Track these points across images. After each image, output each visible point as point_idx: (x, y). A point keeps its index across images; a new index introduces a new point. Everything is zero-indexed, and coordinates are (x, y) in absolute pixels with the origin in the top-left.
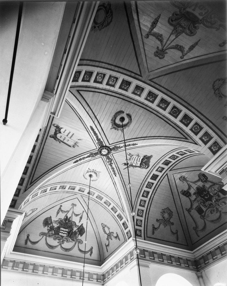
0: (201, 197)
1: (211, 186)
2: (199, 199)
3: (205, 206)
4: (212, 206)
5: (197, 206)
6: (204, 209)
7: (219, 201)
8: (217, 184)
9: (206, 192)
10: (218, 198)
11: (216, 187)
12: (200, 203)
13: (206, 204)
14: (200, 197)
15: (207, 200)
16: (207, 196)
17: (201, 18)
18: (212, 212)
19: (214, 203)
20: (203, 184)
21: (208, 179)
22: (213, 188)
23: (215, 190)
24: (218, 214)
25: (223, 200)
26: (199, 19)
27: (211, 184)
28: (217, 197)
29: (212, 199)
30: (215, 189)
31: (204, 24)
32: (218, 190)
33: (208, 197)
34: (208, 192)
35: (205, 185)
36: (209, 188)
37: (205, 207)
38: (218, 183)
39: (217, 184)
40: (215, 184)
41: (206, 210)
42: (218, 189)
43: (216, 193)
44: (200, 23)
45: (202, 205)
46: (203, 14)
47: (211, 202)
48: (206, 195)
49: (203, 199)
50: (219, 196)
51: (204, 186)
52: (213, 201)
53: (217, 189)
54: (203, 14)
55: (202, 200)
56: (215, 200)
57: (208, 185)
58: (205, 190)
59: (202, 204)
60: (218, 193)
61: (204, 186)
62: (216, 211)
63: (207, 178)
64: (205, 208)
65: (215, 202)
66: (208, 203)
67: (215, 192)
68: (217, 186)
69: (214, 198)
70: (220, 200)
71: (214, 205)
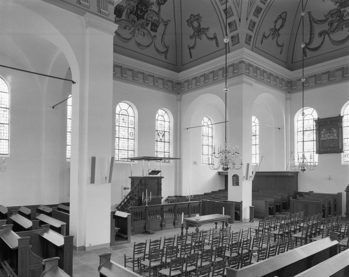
0: (137, 6)
1: (154, 12)
2: (133, 5)
3: (128, 16)
4: (133, 23)
5: (123, 6)
6: (124, 17)
7: (143, 28)
8: (159, 17)
9: (145, 9)
10: (145, 26)
11: (155, 18)
12: (128, 8)
13: (131, 16)
14: (136, 4)
15: (136, 14)
16: (141, 12)
17: (342, 10)
18: (127, 28)
19: (138, 24)
20: (155, 2)
21: (162, 7)
22: (153, 15)
23: (152, 18)
24: (129, 36)
25: (145, 31)
26: (342, 8)
27: (157, 10)
28: (145, 24)
29: (140, 20)
30: (152, 17)
31: (335, 9)
32: (152, 21)
33: (141, 14)
34: (147, 11)
35: (153, 4)
36: (150, 10)
37: (127, 15)
38: (160, 17)
39: (159, 17)
40: (158, 15)
41: (123, 20)
42: (154, 20)
43: (149, 21)
44: (338, 7)
45: (127, 10)
46: (344, 13)
47: (136, 19)
48: (142, 11)
49: (135, 9)
50: (147, 24)
51: (153, 4)
52: (139, 22)
53: (153, 20)
54: (344, 13)
55: (134, 9)
56: (141, 23)
57: (155, 8)
58: (147, 7)
59: (129, 11)
60: (150, 22)
61: (153, 4)
62: (131, 32)
63: (163, 4)
64: (126, 16)
65: (139, 25)
66: (132, 16)
67: (150, 19)
68: (157, 18)
69: (143, 21)
70: (144, 29)
71: (135, 25)
